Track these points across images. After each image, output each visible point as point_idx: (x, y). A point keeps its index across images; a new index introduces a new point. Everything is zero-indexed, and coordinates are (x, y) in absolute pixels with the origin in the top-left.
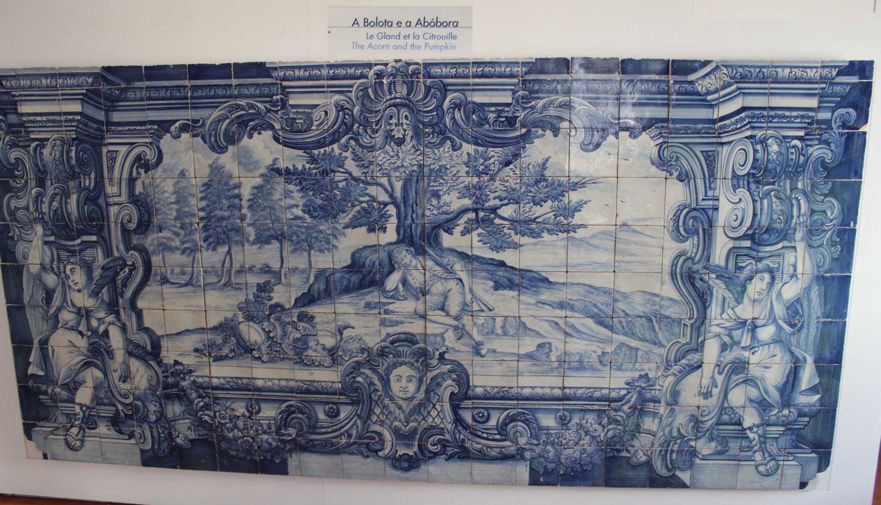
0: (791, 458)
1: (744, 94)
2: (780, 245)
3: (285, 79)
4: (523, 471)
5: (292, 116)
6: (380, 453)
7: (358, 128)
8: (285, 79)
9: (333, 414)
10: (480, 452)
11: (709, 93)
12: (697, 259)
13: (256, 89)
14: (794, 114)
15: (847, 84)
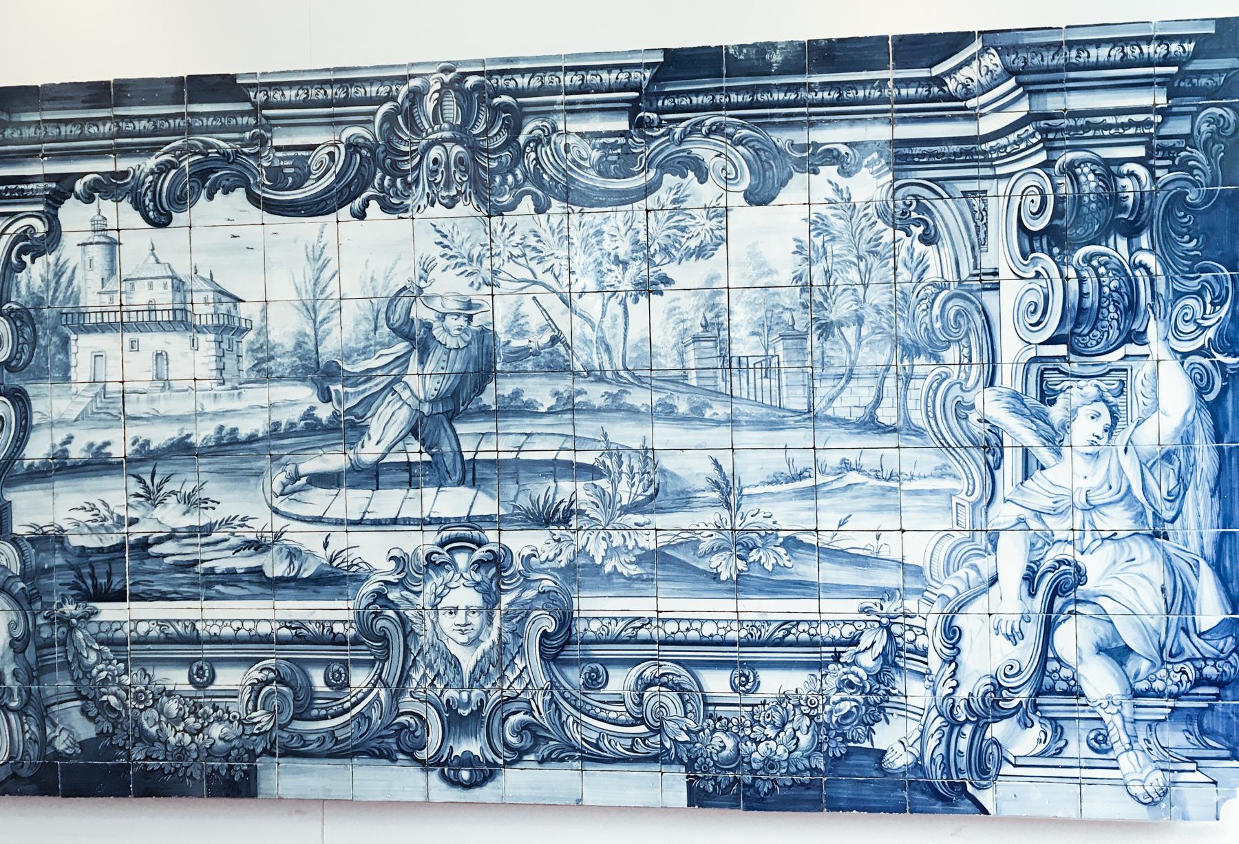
0: (1193, 766)
1: (1031, 93)
2: (1120, 353)
3: (268, 105)
4: (675, 784)
5: (277, 163)
6: (422, 755)
7: (382, 179)
8: (268, 105)
9: (339, 684)
10: (597, 746)
11: (969, 95)
12: (970, 384)
13: (215, 120)
14: (1124, 119)
15: (1219, 72)
